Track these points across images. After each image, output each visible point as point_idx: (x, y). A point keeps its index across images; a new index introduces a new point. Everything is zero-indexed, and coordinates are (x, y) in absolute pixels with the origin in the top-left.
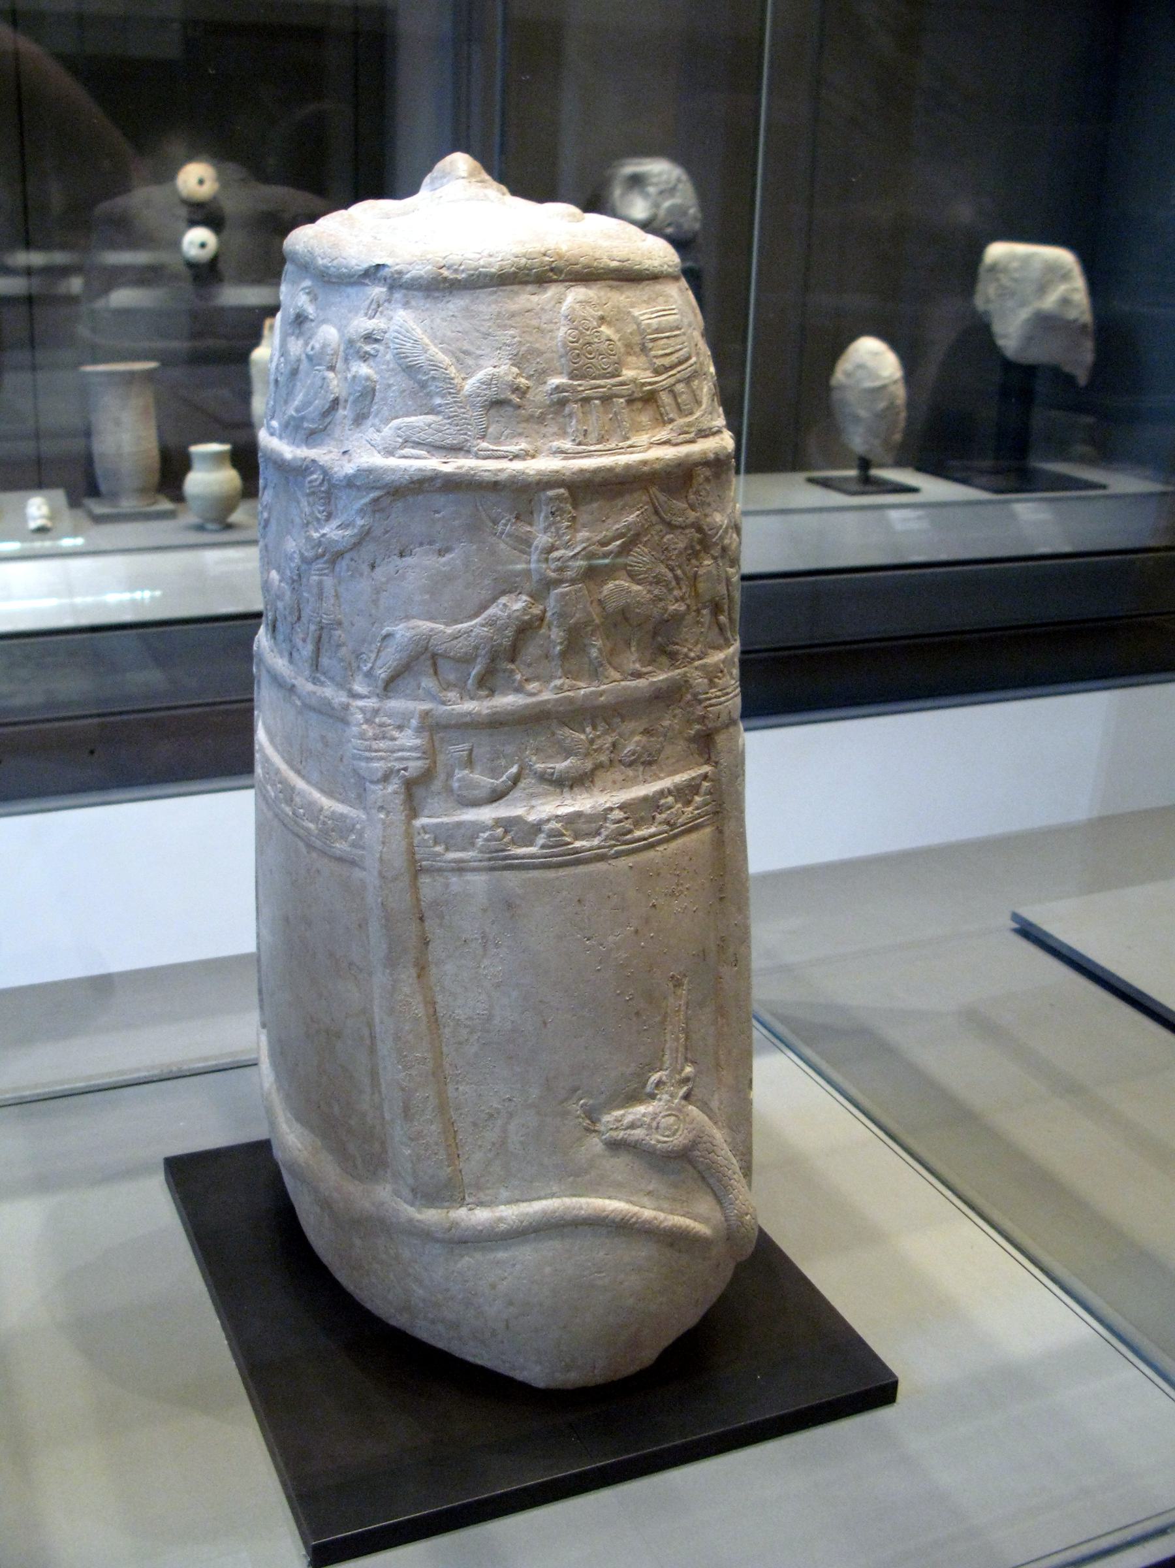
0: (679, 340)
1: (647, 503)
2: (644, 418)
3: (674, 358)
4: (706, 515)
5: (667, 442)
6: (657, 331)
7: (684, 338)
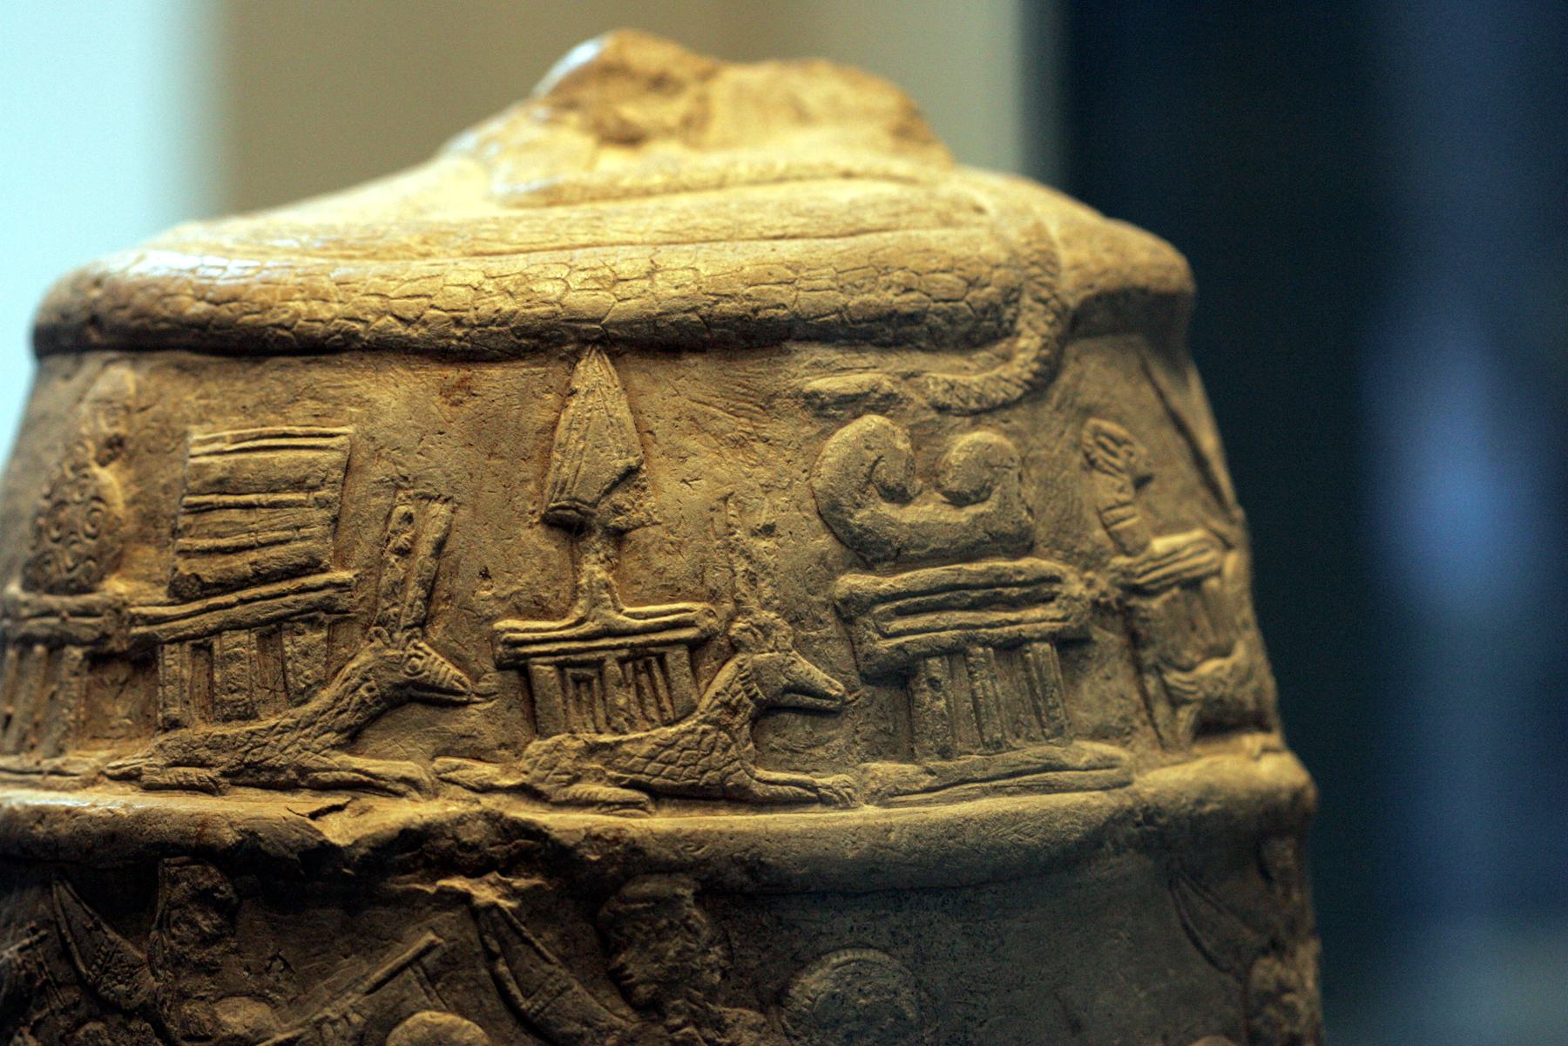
0: (280, 517)
1: (47, 923)
2: (120, 710)
3: (241, 564)
4: (184, 996)
5: (128, 777)
6: (221, 486)
7: (319, 514)
